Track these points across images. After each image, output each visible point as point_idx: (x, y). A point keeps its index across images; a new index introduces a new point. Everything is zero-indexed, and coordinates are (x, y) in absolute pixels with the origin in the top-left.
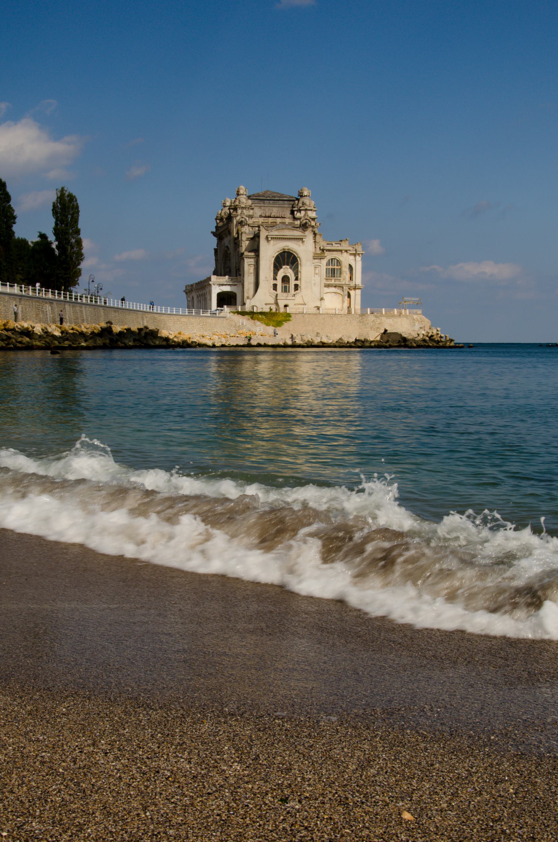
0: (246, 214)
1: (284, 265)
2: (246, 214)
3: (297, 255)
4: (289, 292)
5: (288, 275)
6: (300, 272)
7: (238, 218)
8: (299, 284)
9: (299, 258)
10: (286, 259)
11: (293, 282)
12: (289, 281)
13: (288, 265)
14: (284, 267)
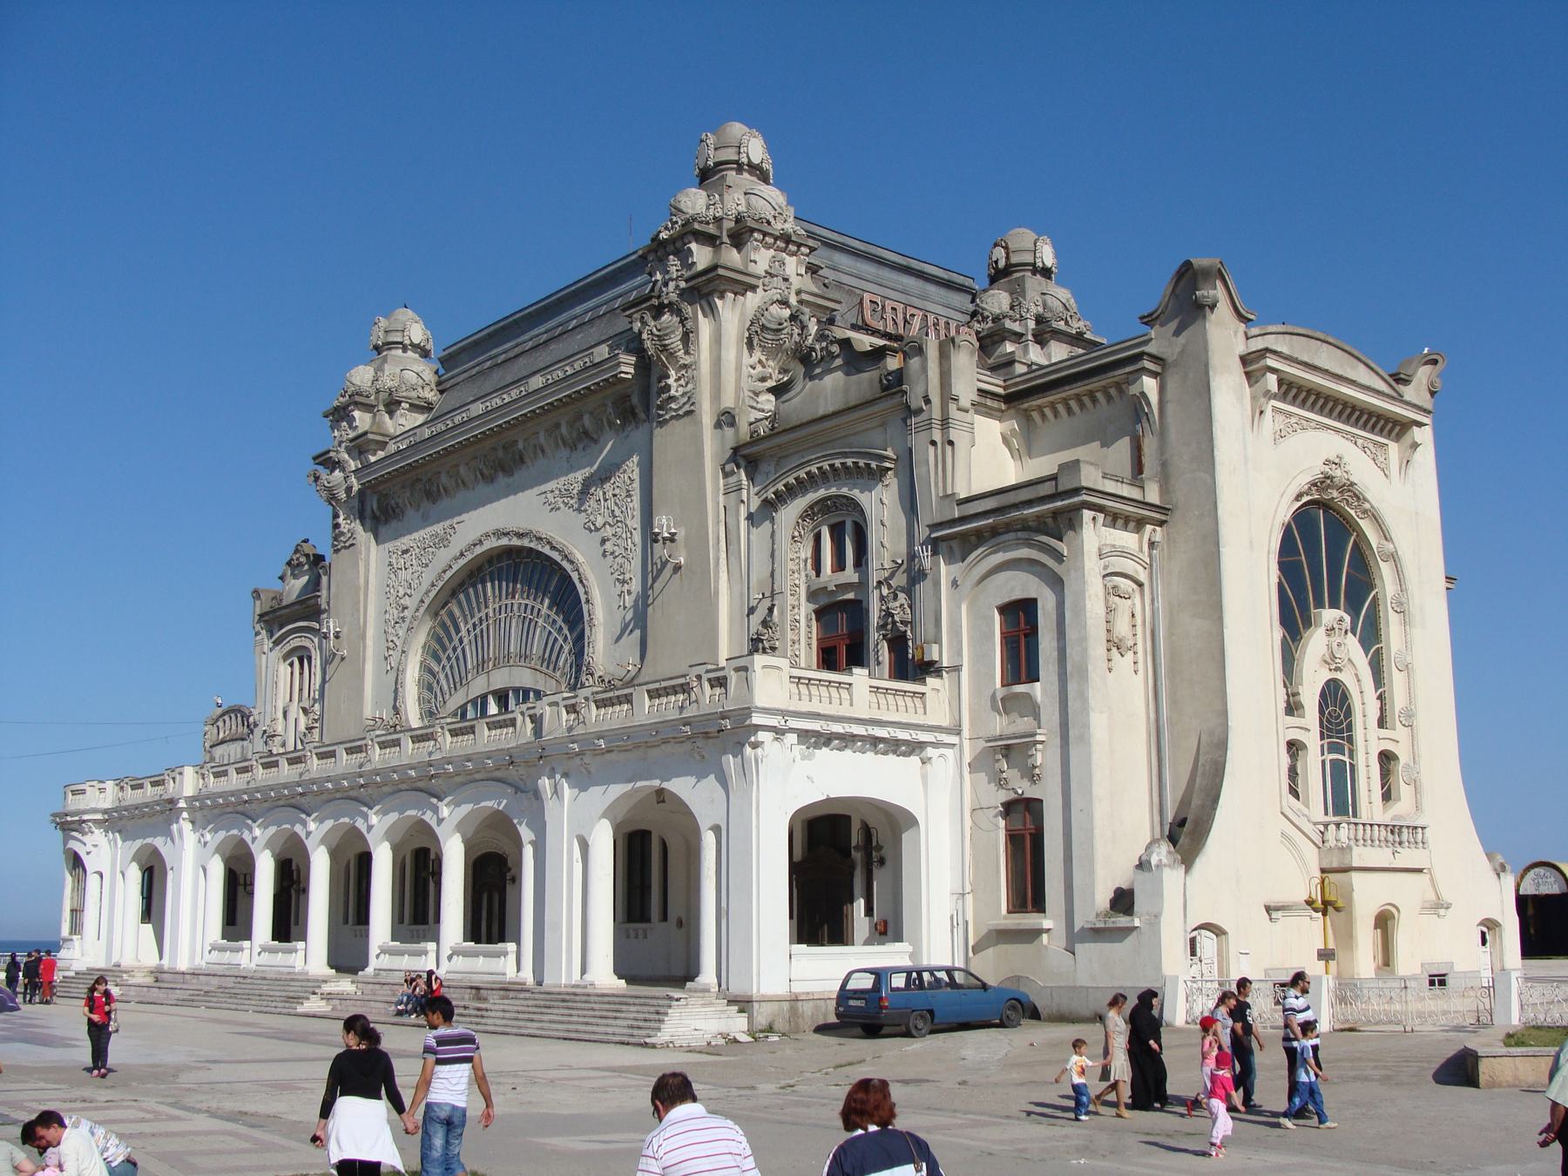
0: (796, 283)
1: (1319, 604)
2: (796, 283)
3: (1386, 536)
4: (1355, 815)
5: (1346, 678)
6: (1406, 668)
7: (753, 300)
8: (1402, 752)
9: (1393, 557)
10: (1326, 557)
11: (1368, 740)
12: (1350, 728)
13: (1334, 604)
14: (1329, 615)
